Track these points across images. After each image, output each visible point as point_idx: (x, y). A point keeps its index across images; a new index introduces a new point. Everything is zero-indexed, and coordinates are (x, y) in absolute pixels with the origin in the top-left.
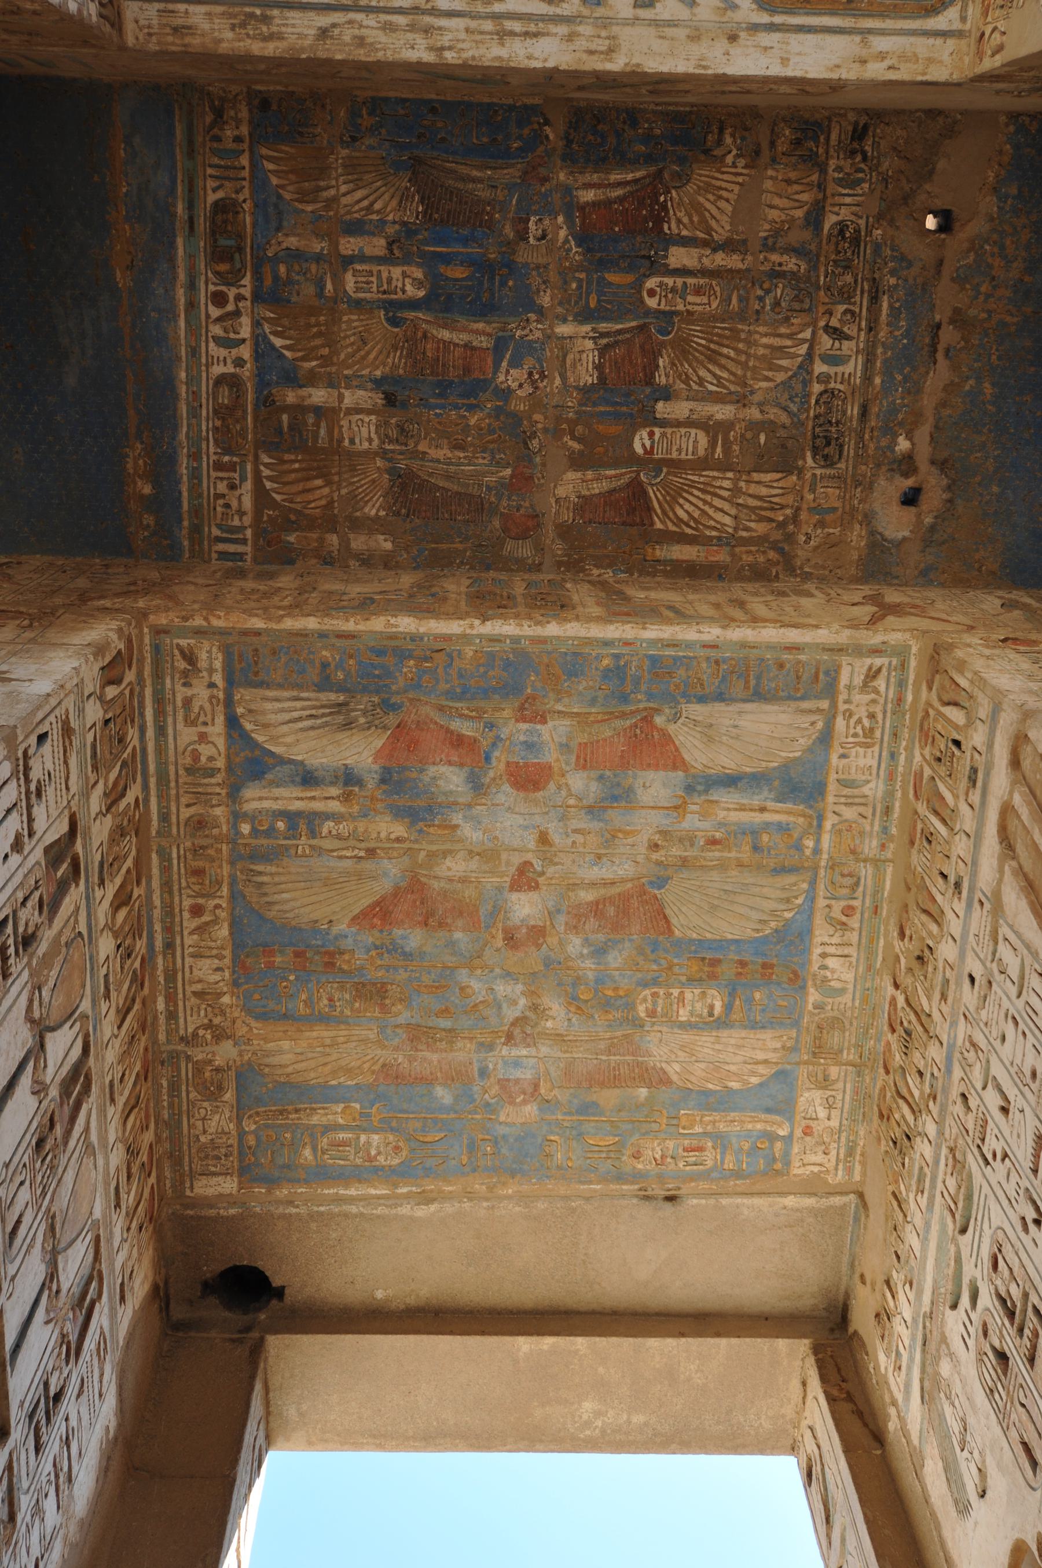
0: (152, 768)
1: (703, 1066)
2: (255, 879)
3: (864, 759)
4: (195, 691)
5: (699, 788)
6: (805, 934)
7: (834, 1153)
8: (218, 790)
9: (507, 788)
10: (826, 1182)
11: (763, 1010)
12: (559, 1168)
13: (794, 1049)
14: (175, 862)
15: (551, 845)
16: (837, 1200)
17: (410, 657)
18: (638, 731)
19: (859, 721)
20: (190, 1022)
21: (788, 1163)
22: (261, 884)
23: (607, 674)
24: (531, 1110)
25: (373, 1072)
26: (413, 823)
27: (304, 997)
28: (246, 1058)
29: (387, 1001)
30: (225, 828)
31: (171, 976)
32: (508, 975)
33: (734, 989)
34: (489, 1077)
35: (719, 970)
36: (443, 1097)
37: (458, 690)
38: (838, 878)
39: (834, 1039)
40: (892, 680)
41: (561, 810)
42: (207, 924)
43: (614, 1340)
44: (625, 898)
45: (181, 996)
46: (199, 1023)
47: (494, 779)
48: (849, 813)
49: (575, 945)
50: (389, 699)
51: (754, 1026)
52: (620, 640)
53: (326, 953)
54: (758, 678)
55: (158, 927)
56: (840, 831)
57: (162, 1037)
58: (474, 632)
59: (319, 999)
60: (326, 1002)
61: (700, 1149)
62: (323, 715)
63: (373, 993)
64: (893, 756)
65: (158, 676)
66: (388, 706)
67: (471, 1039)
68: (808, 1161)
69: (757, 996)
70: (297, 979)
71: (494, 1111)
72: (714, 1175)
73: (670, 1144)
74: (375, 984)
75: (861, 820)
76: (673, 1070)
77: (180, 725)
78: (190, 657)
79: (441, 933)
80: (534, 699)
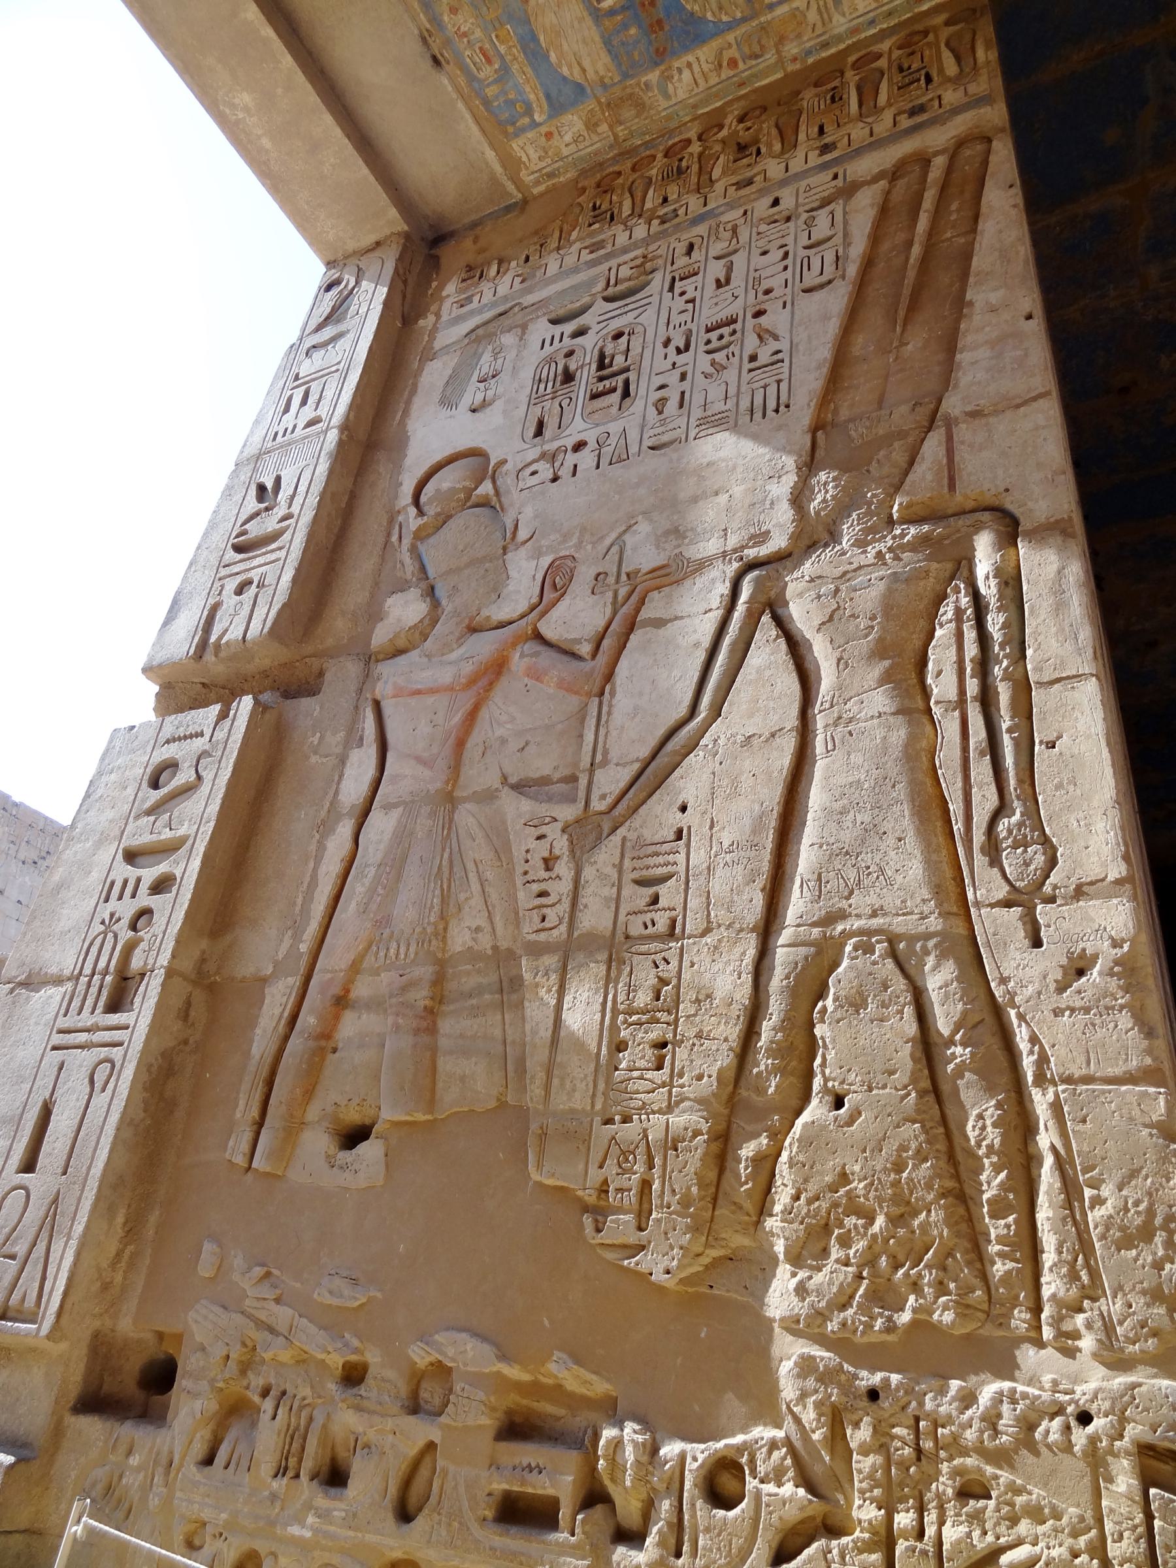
1: (555, 21)
6: (699, 39)
7: (544, 164)
11: (623, 44)
13: (604, 86)
16: (511, 187)
21: (516, 135)
39: (628, 113)
43: (309, 87)
48: (812, 16)
51: (607, 43)
56: (795, 16)
61: (489, 61)
64: (872, 22)
68: (528, 150)
69: (633, 31)
72: (476, 85)
73: (478, 33)
75: (810, 29)
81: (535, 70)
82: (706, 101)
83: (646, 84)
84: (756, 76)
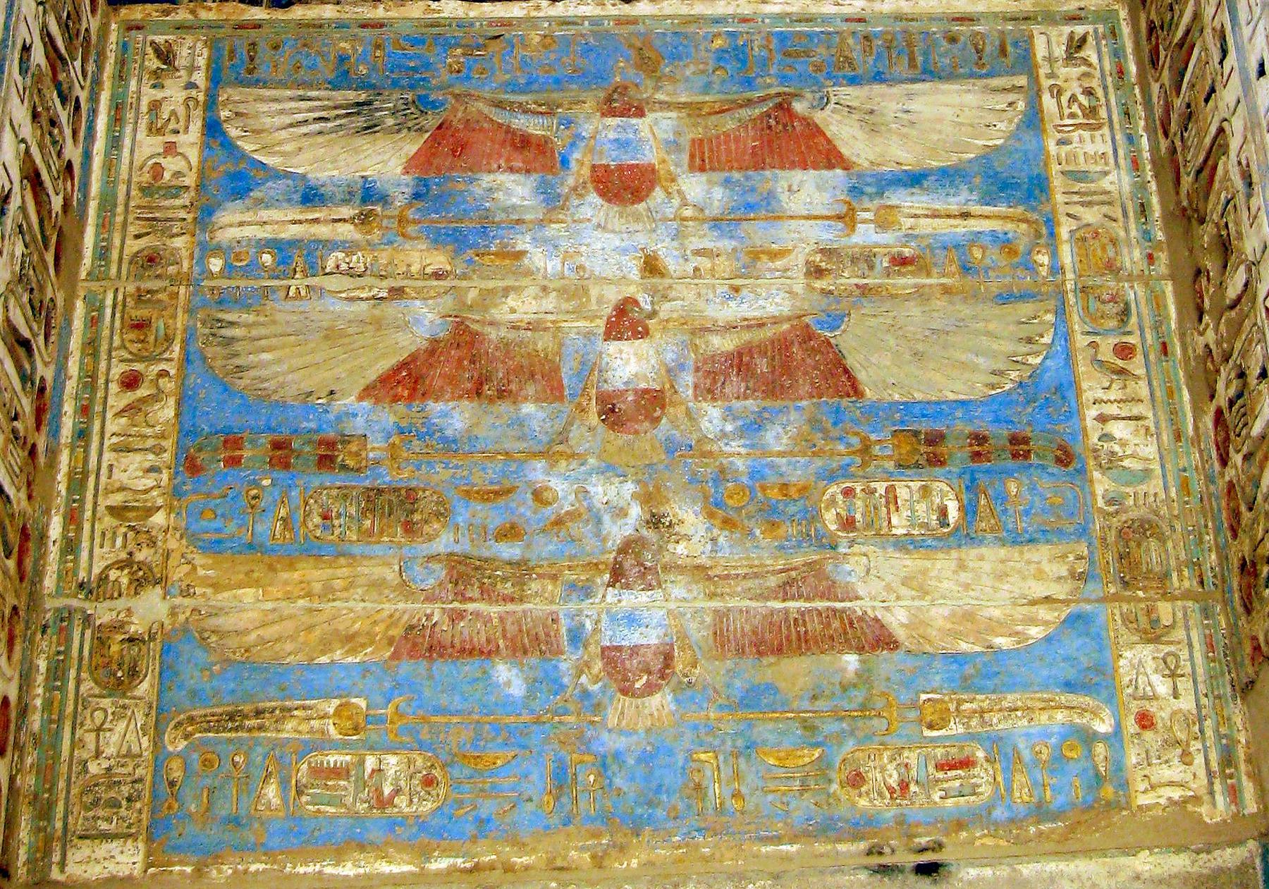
0: (95, 188)
2: (224, 332)
3: (1092, 146)
4: (167, 93)
5: (869, 190)
7: (1199, 760)
8: (182, 214)
9: (594, 198)
10: (1199, 819)
11: (1027, 513)
12: (721, 810)
14: (108, 311)
15: (662, 275)
17: (458, 45)
18: (772, 122)
19: (1073, 99)
20: (97, 557)
21: (1124, 785)
22: (231, 341)
23: (721, 54)
24: (661, 702)
25: (391, 641)
26: (457, 252)
27: (283, 513)
28: (182, 618)
29: (417, 517)
30: (186, 265)
31: (78, 482)
32: (609, 470)
33: (973, 480)
34: (585, 647)
35: (942, 449)
36: (508, 684)
37: (522, 81)
38: (1094, 305)
39: (1151, 554)
40: (1104, 50)
41: (675, 225)
42: (143, 400)
44: (782, 346)
45: (88, 514)
46: (112, 558)
47: (575, 189)
48: (1091, 216)
49: (712, 417)
50: (427, 96)
51: (1018, 540)
52: (733, 16)
53: (320, 443)
54: (926, 53)
55: (68, 407)
56: (1084, 239)
57: (49, 582)
58: (541, 14)
59: (307, 515)
60: (318, 520)
61: (966, 763)
62: (337, 117)
63: (399, 508)
64: (1130, 139)
65: (121, 77)
66: (423, 104)
67: (554, 578)
69: (1013, 487)
70: (273, 485)
71: (598, 708)
73: (912, 757)
74: (396, 490)
76: (897, 619)
77: (142, 135)
78: (166, 55)
79: (504, 407)
80: (626, 88)
81: (1012, 688)
82: (1174, 414)
83: (1110, 502)
84: (1159, 324)
